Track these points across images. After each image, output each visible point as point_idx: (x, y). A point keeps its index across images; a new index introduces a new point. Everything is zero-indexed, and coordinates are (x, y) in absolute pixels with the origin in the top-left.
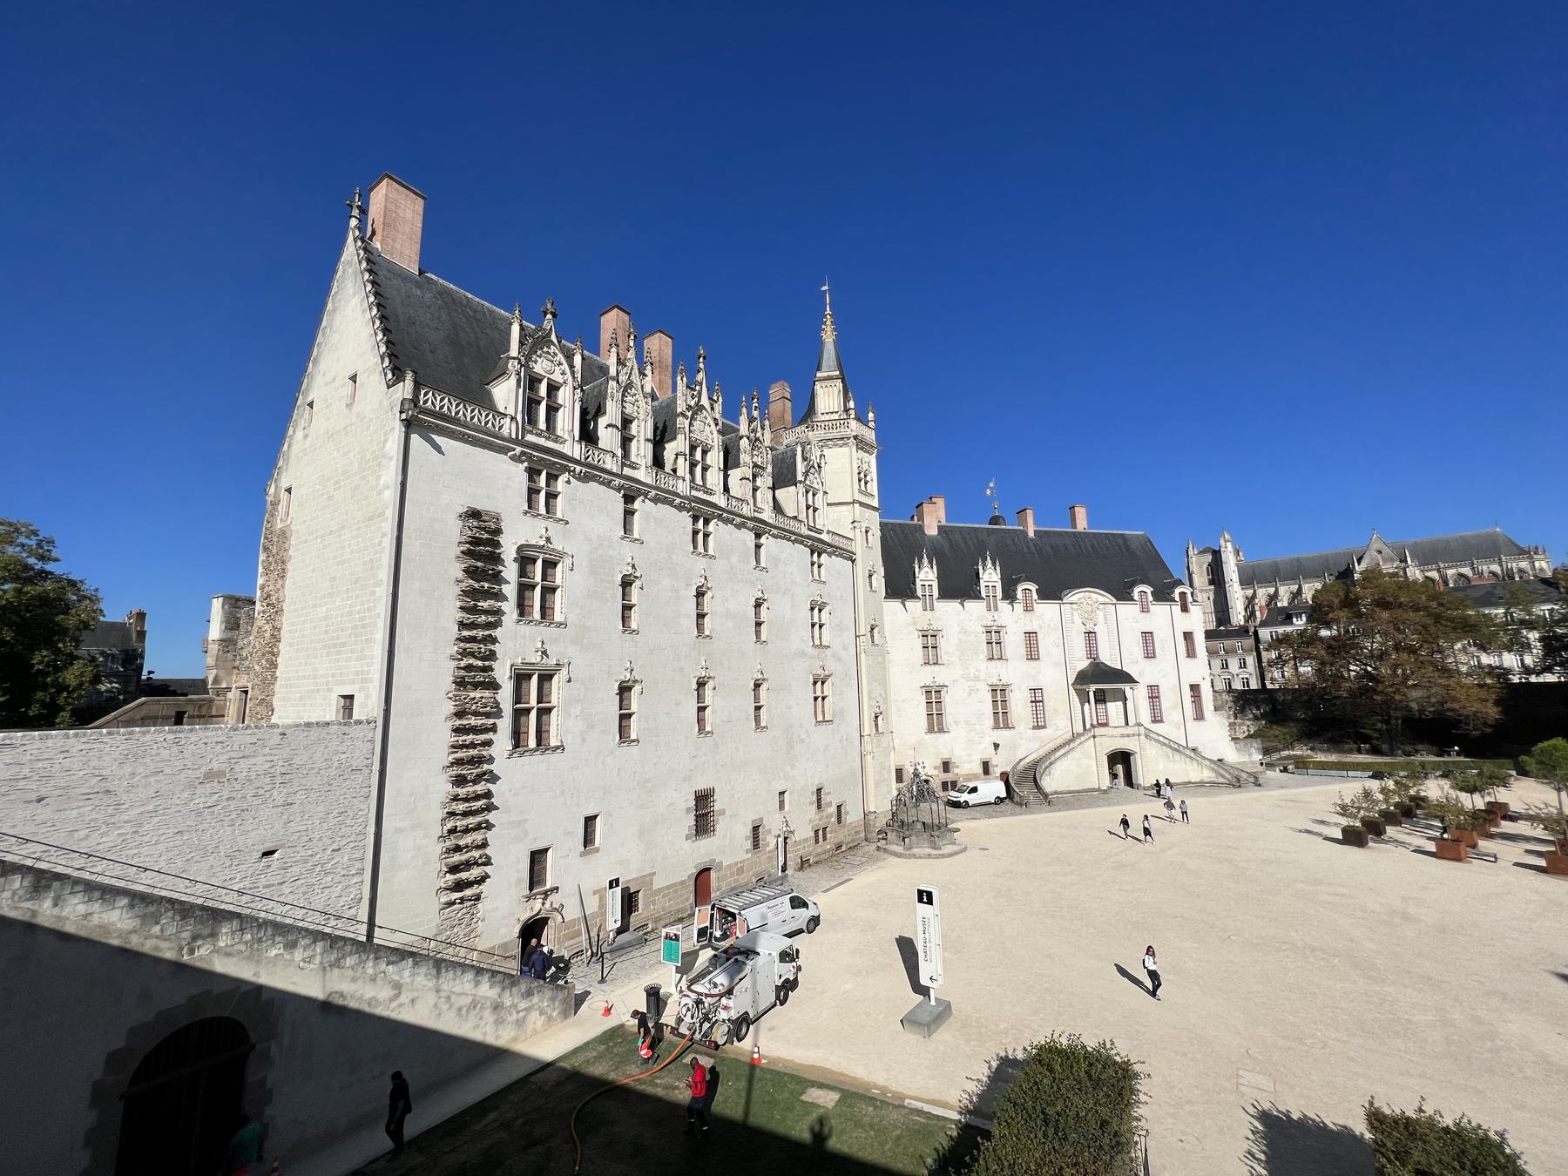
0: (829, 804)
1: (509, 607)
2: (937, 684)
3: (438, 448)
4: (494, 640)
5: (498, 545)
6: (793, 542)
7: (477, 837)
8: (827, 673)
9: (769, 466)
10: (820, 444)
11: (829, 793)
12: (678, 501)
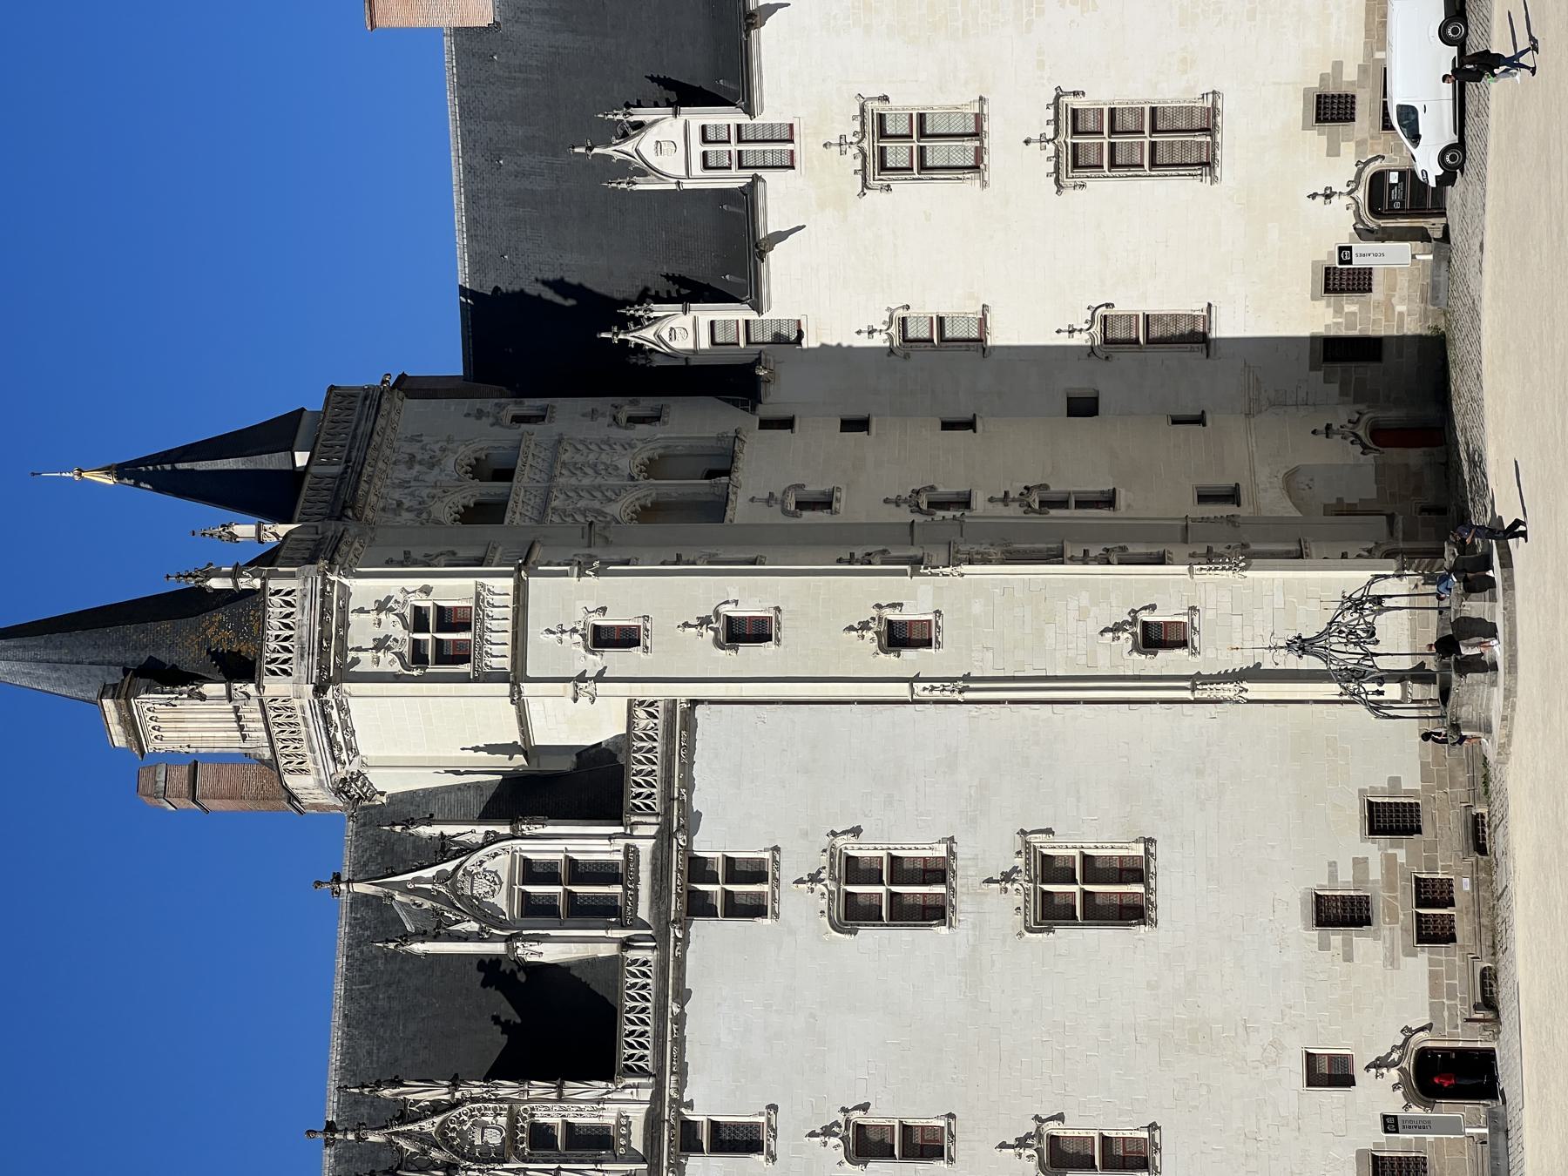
0: (1360, 864)
2: (1050, 135)
6: (683, 996)
8: (1020, 862)
9: (502, 1092)
10: (344, 757)
11: (1333, 876)
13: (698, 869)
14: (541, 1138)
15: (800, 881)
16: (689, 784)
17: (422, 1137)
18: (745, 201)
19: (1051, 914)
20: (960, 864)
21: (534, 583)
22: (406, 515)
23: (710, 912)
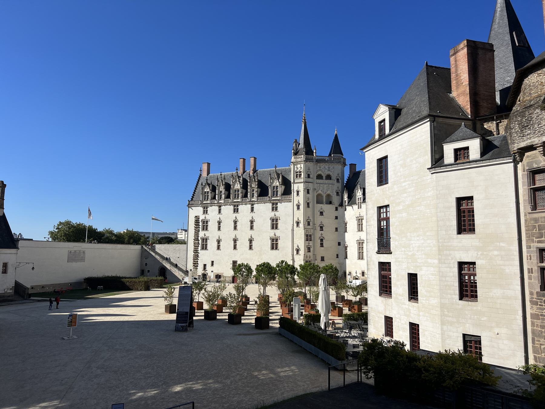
1: (200, 229)
2: (361, 240)
3: (192, 209)
4: (199, 234)
5: (199, 220)
6: (264, 203)
7: (197, 260)
12: (228, 204)
13: (277, 204)
14: (253, 190)
15: (275, 214)
16: (284, 202)
17: (253, 179)
18: (355, 203)
19: (272, 240)
20: (276, 230)
21: (303, 184)
22: (319, 169)
23: (273, 205)
